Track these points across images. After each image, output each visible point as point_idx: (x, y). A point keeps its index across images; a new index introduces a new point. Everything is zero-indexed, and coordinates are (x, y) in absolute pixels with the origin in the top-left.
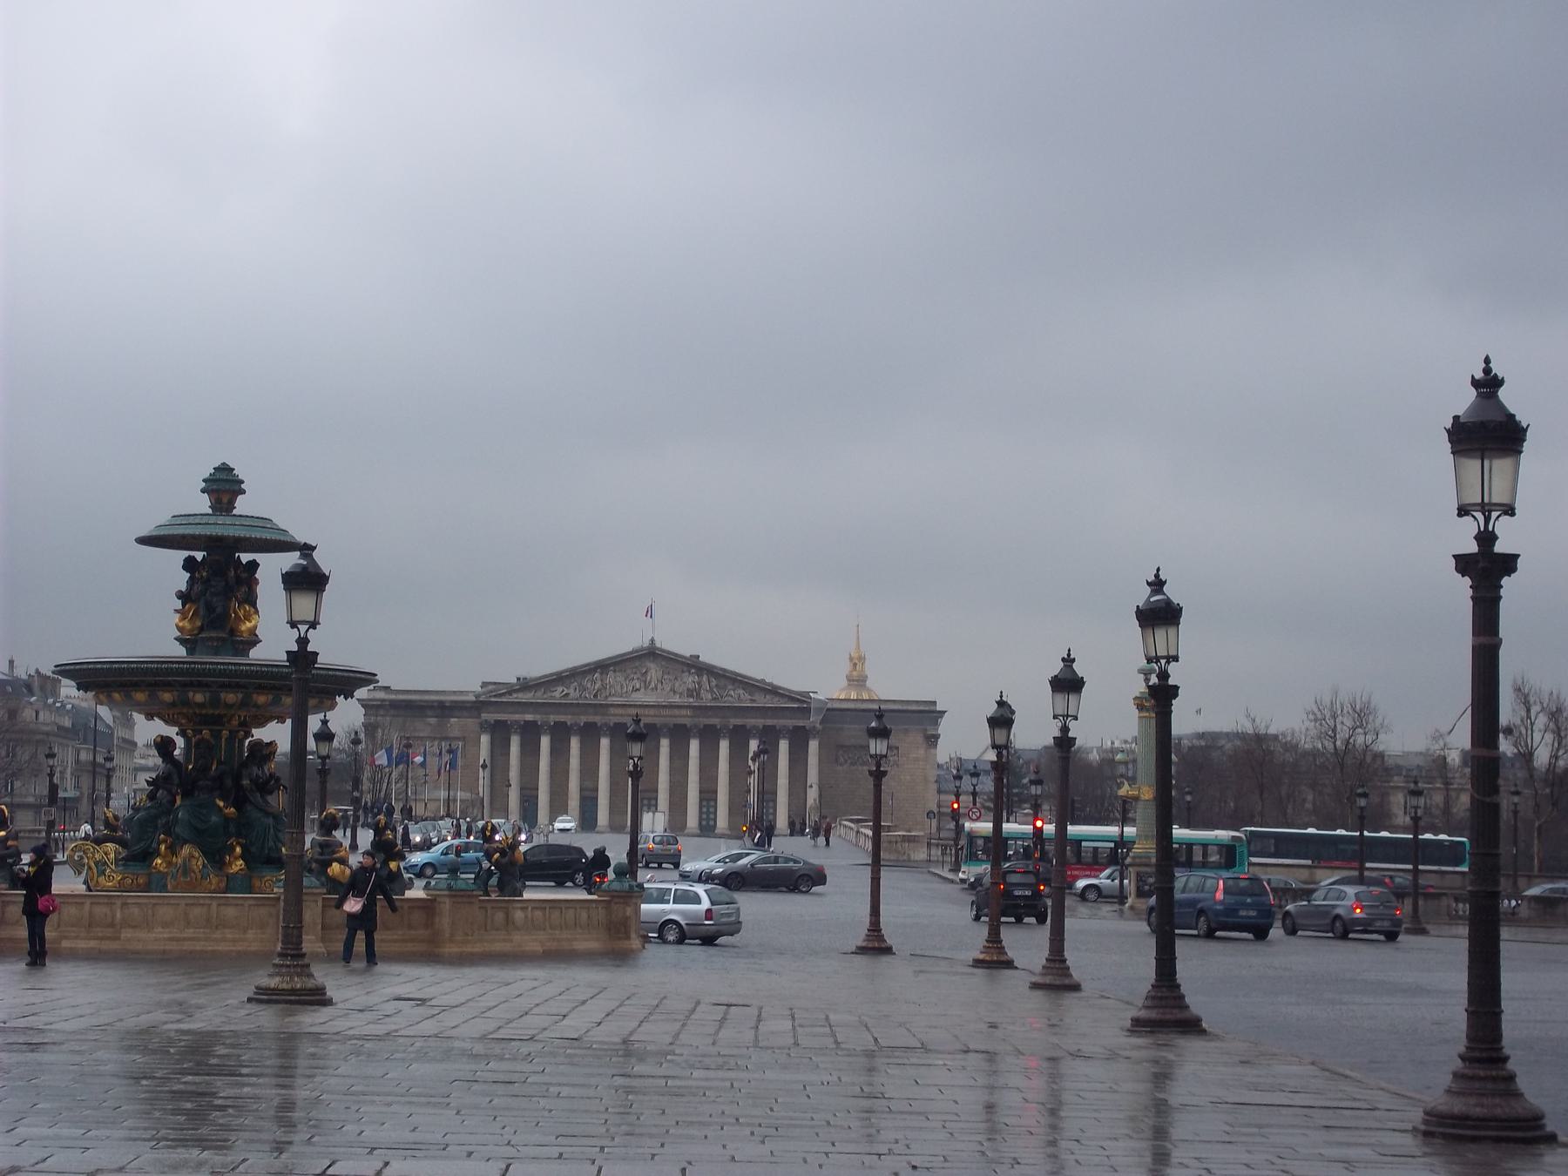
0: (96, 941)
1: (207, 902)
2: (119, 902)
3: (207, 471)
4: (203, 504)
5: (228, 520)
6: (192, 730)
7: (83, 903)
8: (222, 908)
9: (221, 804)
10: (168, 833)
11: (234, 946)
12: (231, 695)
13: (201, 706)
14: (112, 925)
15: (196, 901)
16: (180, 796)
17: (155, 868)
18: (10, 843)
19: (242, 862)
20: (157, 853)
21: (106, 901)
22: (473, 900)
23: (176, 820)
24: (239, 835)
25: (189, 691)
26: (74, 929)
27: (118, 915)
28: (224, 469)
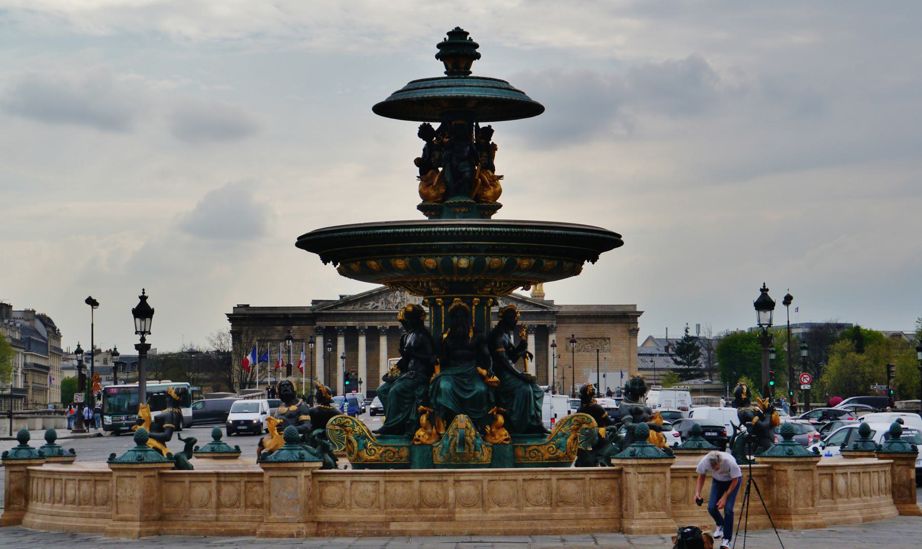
0: (428, 523)
1: (547, 477)
2: (451, 479)
3: (442, 37)
4: (438, 70)
5: (467, 82)
6: (443, 299)
7: (410, 481)
8: (562, 482)
9: (484, 372)
11: (578, 524)
12: (496, 259)
13: (463, 271)
14: (445, 504)
15: (534, 477)
16: (439, 366)
17: (418, 440)
18: (304, 417)
19: (506, 431)
21: (437, 478)
22: (811, 467)
23: (438, 391)
24: (498, 404)
25: (453, 256)
26: (402, 510)
27: (451, 493)
28: (458, 35)
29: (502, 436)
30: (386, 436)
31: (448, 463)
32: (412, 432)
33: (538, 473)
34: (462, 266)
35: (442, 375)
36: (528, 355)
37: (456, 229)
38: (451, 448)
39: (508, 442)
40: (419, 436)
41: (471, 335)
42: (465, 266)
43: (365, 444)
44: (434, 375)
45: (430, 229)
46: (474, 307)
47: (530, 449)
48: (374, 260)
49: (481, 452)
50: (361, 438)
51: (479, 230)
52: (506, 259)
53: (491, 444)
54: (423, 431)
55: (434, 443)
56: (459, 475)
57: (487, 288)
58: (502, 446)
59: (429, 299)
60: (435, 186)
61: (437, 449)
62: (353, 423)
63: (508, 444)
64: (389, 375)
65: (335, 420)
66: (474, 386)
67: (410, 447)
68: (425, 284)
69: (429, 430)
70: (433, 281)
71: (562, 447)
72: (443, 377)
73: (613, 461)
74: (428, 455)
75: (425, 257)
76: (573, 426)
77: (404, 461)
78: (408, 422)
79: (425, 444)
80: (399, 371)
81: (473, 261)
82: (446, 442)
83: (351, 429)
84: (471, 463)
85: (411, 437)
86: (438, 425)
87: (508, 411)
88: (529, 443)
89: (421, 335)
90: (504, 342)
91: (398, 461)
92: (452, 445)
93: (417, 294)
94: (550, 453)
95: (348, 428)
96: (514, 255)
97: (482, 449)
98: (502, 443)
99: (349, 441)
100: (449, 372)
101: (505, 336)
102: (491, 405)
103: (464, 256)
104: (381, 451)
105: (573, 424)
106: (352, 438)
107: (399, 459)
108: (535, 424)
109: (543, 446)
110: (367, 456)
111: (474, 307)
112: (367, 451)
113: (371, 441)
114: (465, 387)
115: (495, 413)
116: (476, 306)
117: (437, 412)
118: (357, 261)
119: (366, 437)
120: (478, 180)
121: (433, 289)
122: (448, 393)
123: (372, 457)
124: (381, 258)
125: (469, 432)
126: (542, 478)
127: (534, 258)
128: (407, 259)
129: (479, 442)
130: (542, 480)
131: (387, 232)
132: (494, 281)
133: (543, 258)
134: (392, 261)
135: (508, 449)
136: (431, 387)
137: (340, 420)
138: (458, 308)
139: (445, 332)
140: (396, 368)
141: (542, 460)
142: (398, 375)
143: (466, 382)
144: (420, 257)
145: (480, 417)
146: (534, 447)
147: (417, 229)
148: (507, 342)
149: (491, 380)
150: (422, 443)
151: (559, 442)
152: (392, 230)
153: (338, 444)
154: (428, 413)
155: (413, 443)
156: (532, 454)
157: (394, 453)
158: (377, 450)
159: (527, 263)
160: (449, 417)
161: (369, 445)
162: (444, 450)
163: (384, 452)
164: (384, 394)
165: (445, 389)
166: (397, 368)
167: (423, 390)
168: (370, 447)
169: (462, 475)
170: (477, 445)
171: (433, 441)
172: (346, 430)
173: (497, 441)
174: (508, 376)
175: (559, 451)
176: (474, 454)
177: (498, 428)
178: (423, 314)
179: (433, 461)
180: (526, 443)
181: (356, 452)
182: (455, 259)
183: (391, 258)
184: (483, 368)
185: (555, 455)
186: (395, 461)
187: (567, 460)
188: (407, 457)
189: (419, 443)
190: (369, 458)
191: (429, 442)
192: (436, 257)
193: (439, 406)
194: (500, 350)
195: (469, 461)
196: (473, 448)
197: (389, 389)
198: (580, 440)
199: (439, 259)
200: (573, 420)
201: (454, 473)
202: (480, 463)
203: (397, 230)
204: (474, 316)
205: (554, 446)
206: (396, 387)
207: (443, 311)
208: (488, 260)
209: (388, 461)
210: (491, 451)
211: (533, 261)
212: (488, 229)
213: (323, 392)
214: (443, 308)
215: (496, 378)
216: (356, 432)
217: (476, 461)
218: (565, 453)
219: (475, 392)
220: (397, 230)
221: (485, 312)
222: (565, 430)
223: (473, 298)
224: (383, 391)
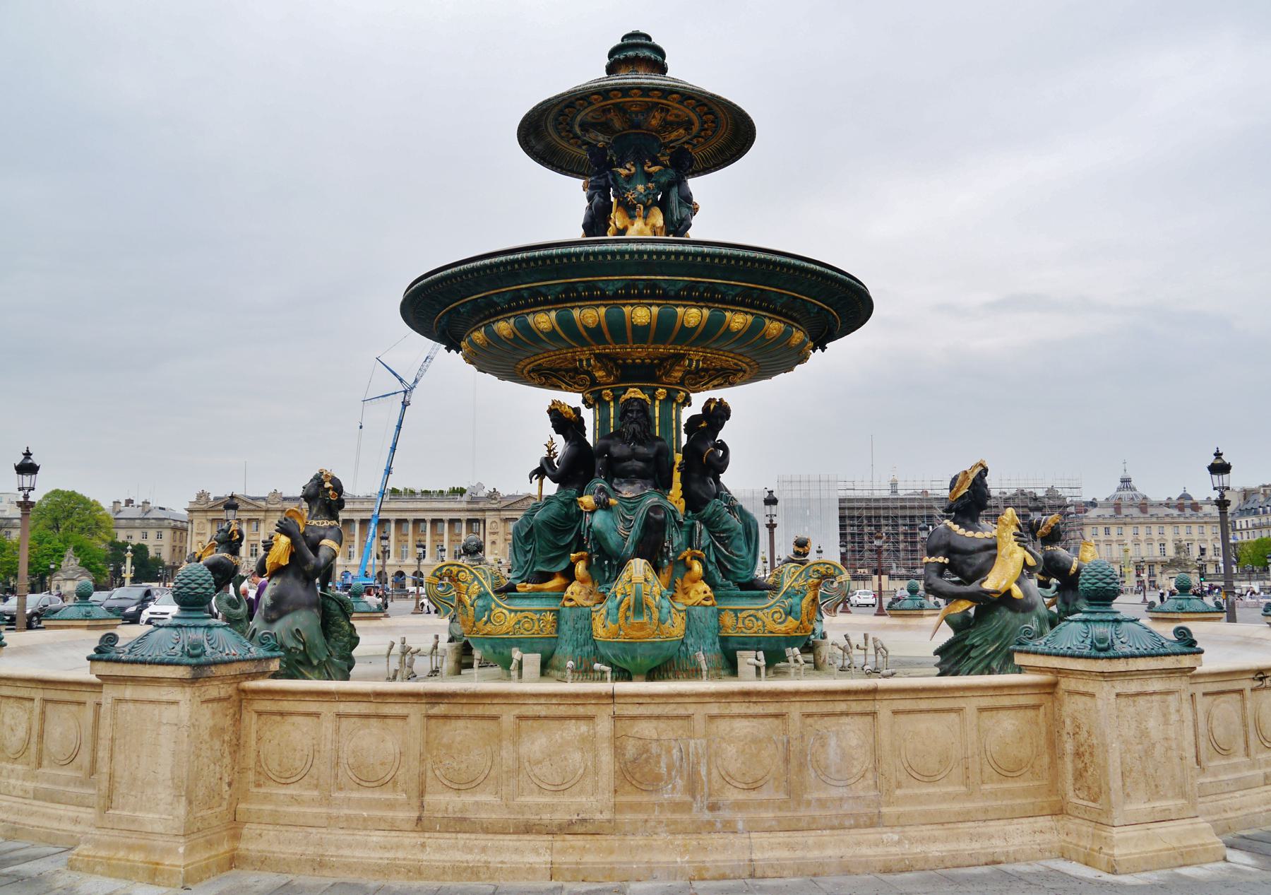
12: (694, 311)
13: (641, 333)
17: (571, 600)
20: (569, 575)
39: (709, 603)
46: (657, 403)
47: (745, 614)
53: (684, 608)
57: (679, 371)
59: (591, 393)
67: (557, 612)
68: (585, 363)
70: (598, 357)
73: (1019, 659)
75: (580, 307)
76: (812, 580)
79: (582, 606)
82: (610, 604)
91: (538, 634)
92: (622, 610)
105: (811, 577)
109: (766, 611)
111: (657, 403)
115: (688, 559)
116: (660, 401)
118: (481, 327)
121: (597, 375)
128: (553, 314)
129: (665, 603)
134: (530, 319)
141: (764, 633)
146: (752, 612)
159: (742, 320)
160: (619, 564)
177: (695, 582)
183: (528, 314)
186: (533, 634)
198: (822, 599)
200: (811, 571)
207: (612, 410)
214: (612, 404)
223: (656, 389)
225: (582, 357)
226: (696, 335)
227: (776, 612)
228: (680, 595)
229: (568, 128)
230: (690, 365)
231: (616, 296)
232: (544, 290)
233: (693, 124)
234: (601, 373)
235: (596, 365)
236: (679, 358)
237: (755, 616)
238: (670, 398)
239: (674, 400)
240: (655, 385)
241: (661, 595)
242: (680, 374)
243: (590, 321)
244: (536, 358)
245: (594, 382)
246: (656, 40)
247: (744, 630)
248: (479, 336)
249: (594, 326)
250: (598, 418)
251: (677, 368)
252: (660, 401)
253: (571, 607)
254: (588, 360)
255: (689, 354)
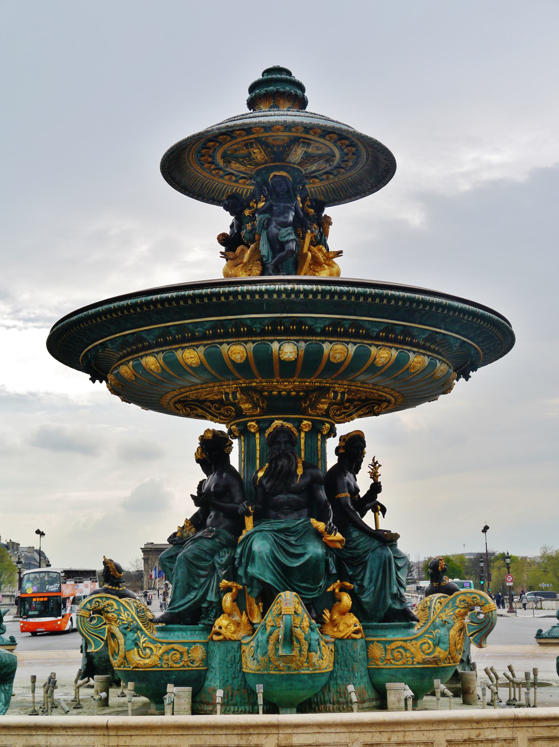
1: (506, 733)
6: (258, 422)
9: (321, 526)
10: (232, 576)
12: (339, 347)
15: (473, 734)
16: (251, 518)
17: (218, 634)
19: (355, 619)
23: (250, 557)
24: (342, 576)
25: (272, 341)
29: (349, 626)
30: (170, 626)
31: (266, 672)
32: (210, 620)
33: (485, 725)
34: (286, 357)
35: (256, 532)
36: (379, 507)
37: (277, 287)
38: (270, 647)
39: (358, 636)
40: (220, 628)
41: (300, 471)
42: (291, 357)
43: (136, 639)
44: (244, 532)
45: (235, 288)
46: (303, 435)
47: (393, 646)
48: (151, 354)
49: (319, 653)
50: (131, 631)
51: (315, 289)
52: (355, 347)
53: (333, 640)
54: (226, 620)
55: (243, 638)
56: (289, 731)
57: (324, 403)
58: (350, 642)
59: (237, 425)
60: (245, 264)
61: (248, 648)
62: (118, 606)
63: (359, 639)
64: (178, 535)
65: (90, 602)
66: (305, 548)
67: (206, 644)
68: (230, 396)
69: (237, 618)
70: (244, 391)
71: (444, 643)
72: (257, 534)
74: (235, 656)
75: (228, 343)
76: (459, 610)
77: (197, 667)
78: (205, 605)
79: (230, 639)
80: (193, 529)
81: (304, 348)
82: (261, 637)
83: (115, 615)
84: (303, 672)
85: (208, 628)
86: (250, 609)
87: (356, 587)
88: (390, 637)
89: (224, 475)
90: (349, 484)
91: (189, 666)
92: (271, 642)
93: (220, 419)
94: (424, 652)
95: (110, 615)
96: (365, 342)
97: (320, 649)
98: (349, 638)
99: (113, 636)
100: (265, 526)
101: (349, 477)
102: (331, 578)
103: (289, 341)
104: (161, 651)
105: (457, 607)
106: (116, 630)
107: (190, 664)
108: (397, 607)
109: (414, 642)
110: (139, 658)
111: (303, 435)
112: (138, 651)
113: (146, 635)
114: (292, 550)
115: (337, 591)
116: (306, 433)
117: (248, 590)
118: (129, 361)
119: (138, 629)
120: (306, 254)
121: (243, 406)
122: (265, 557)
123: (147, 661)
124: (163, 352)
125: (300, 620)
126: (494, 737)
127: (397, 349)
128: (202, 349)
129: (315, 636)
130: (492, 741)
131: (167, 298)
132: (333, 391)
133: (409, 351)
134: (179, 354)
135: (358, 647)
136: (239, 550)
137: (98, 602)
138: (280, 430)
139: (261, 468)
140: (188, 524)
141: (412, 664)
142: (191, 535)
143: (293, 542)
144: (221, 344)
145: (315, 596)
146: (399, 644)
147: (214, 290)
148: (352, 484)
149: (332, 537)
150: (225, 638)
151: (438, 635)
152: (174, 294)
153: (94, 641)
154: (234, 590)
155: (212, 639)
156: (396, 654)
157: (182, 654)
158: (154, 649)
159: (386, 355)
161: (142, 641)
162: (259, 650)
163: (167, 652)
164: (169, 562)
165: (260, 552)
166: (190, 525)
167: (227, 556)
168: (144, 645)
169: (295, 731)
170: (312, 642)
171: (242, 634)
172: (107, 618)
173: (341, 635)
174: (355, 534)
175: (438, 649)
176: (308, 658)
177: (343, 614)
178: (228, 444)
179: (241, 667)
180: (385, 636)
181: (122, 653)
182: (275, 346)
183: (176, 349)
184: (319, 520)
185: (432, 656)
186: (183, 666)
187: (450, 663)
188: (202, 660)
189: (221, 637)
190: (141, 663)
191: (235, 637)
192: (246, 342)
193: (252, 579)
194: (343, 495)
195: (299, 668)
196: (305, 647)
197: (177, 555)
198: (469, 632)
199: (251, 346)
200: (458, 601)
201: (277, 726)
202: (317, 671)
203: (183, 293)
204: (302, 447)
205: (430, 642)
206: (188, 551)
208: (326, 347)
209: (171, 667)
210: (333, 650)
211: (395, 353)
212: (328, 288)
213: (111, 570)
214: (257, 436)
215: (339, 536)
216: (123, 620)
217: (311, 669)
218: (447, 652)
219: (307, 557)
220: (183, 293)
221: (319, 443)
222: (446, 615)
223: (301, 421)
224: (168, 558)
225: (227, 390)
226: (342, 369)
227: (424, 643)
228: (328, 630)
229: (210, 159)
230: (335, 397)
231: (263, 333)
232: (191, 327)
233: (334, 156)
234: (247, 406)
235: (242, 399)
236: (323, 391)
237: (404, 648)
238: (316, 429)
239: (320, 431)
240: (301, 417)
241: (310, 628)
242: (325, 407)
243: (238, 357)
244: (182, 390)
245: (240, 413)
246: (297, 76)
247: (393, 662)
248: (126, 370)
249: (242, 361)
250: (243, 450)
251: (323, 400)
252: (306, 433)
253: (219, 641)
254: (234, 394)
255: (334, 387)
